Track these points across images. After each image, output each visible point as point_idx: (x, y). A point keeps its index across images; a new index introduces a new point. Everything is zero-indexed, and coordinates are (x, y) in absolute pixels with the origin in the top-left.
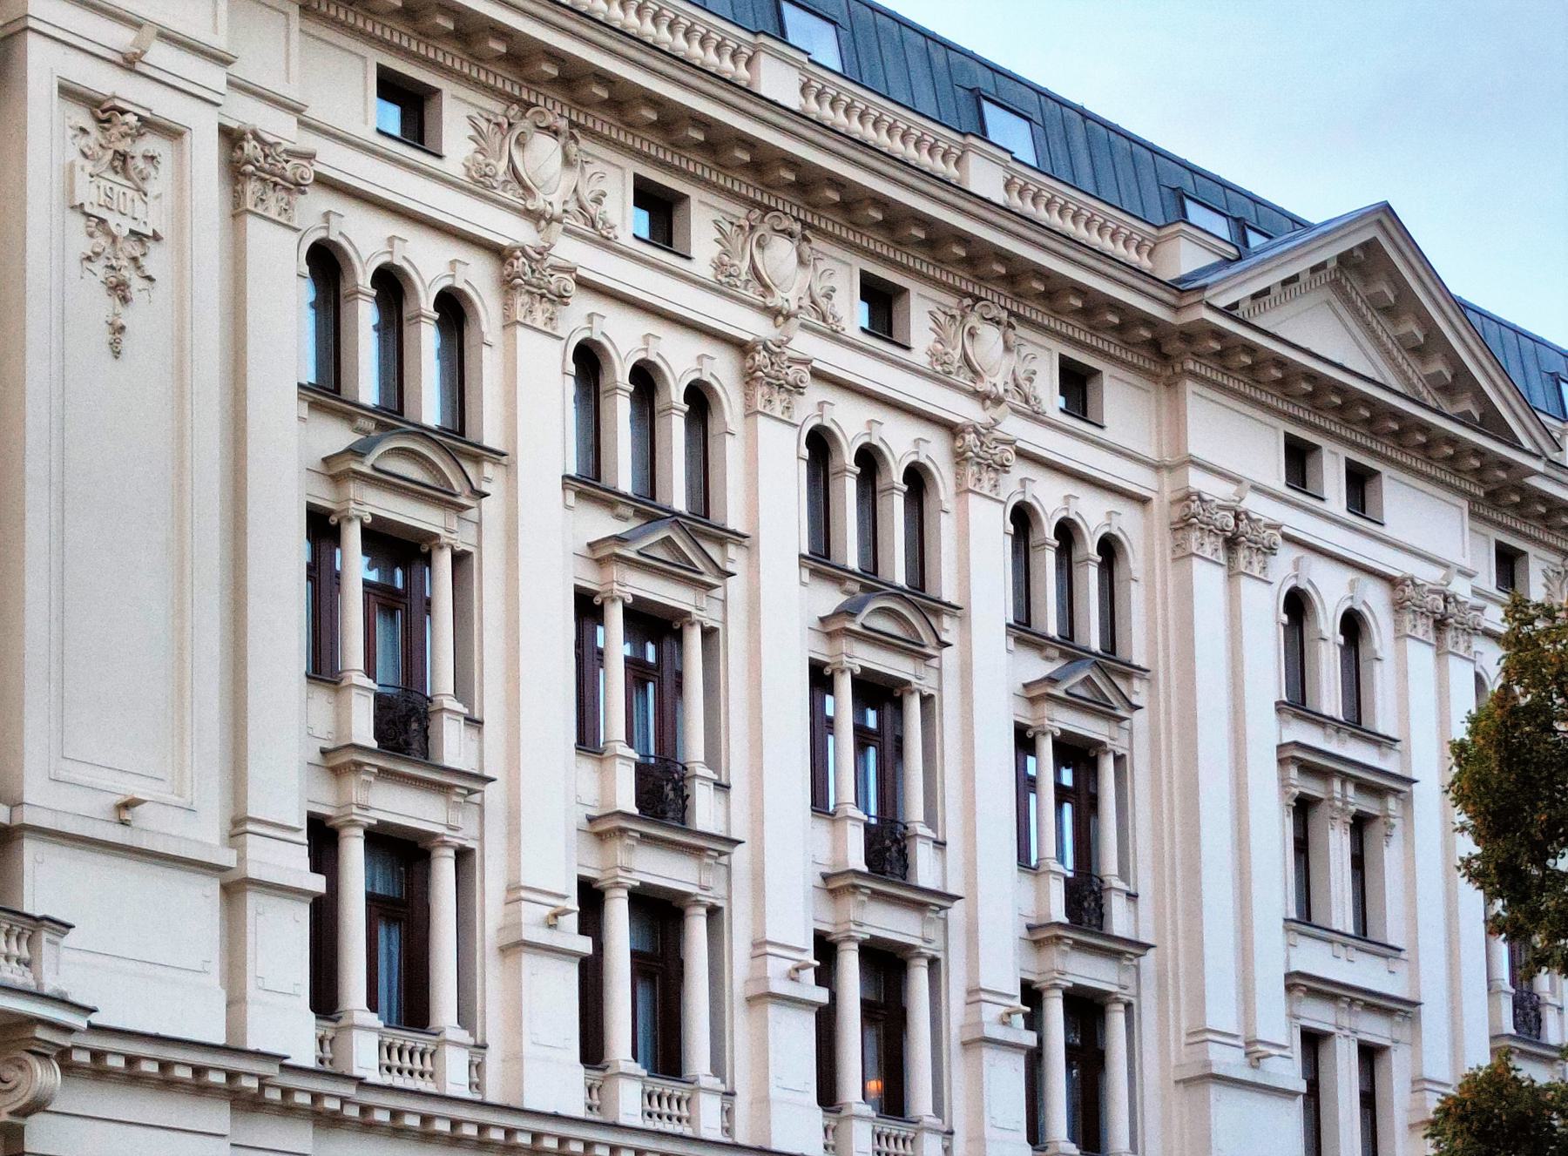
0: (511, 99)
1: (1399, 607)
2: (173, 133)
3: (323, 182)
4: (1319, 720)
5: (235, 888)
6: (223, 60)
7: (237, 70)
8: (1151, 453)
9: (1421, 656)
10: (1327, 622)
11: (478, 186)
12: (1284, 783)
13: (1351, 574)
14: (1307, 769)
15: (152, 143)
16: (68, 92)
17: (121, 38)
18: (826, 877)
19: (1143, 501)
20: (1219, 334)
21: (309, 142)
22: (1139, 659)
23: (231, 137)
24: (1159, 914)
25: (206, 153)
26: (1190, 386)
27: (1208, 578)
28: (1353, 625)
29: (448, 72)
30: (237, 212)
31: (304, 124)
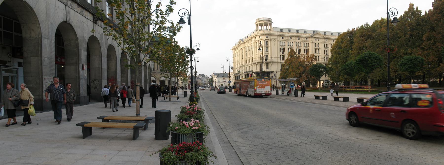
11: (285, 39)
25: (277, 40)
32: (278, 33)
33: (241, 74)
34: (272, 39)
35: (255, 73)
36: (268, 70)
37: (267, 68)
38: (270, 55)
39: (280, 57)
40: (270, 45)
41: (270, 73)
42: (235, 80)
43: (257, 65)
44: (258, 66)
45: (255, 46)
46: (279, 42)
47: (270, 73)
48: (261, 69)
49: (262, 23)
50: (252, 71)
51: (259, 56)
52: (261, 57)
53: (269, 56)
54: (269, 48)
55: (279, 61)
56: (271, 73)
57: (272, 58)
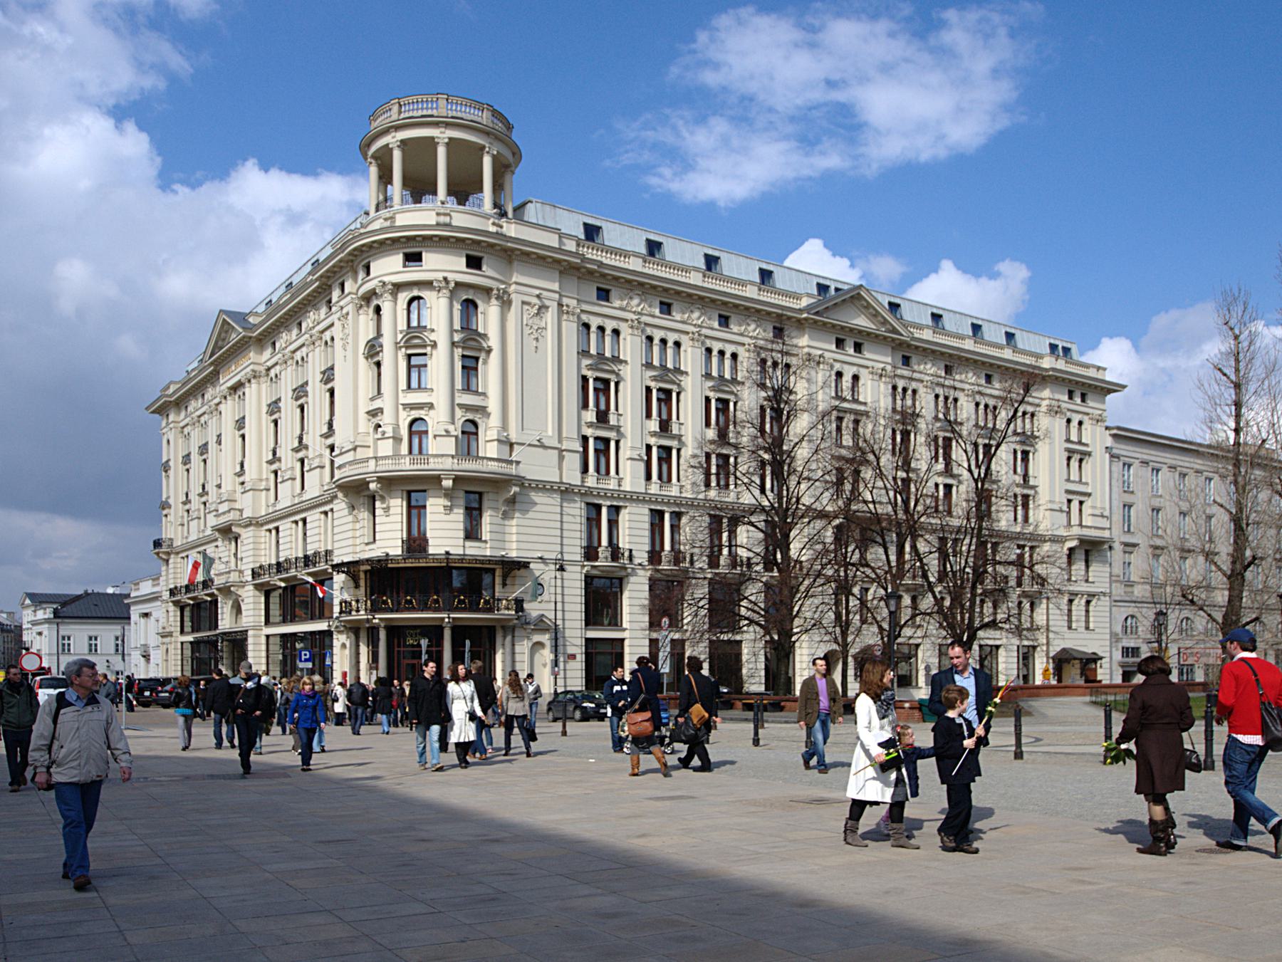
32: (571, 246)
33: (226, 590)
35: (350, 568)
36: (473, 549)
37: (472, 533)
40: (494, 342)
41: (498, 573)
42: (182, 632)
43: (378, 504)
44: (387, 509)
46: (570, 329)
47: (493, 571)
48: (415, 543)
49: (431, 143)
50: (328, 553)
51: (396, 427)
52: (411, 433)
53: (489, 431)
54: (485, 362)
56: (505, 577)
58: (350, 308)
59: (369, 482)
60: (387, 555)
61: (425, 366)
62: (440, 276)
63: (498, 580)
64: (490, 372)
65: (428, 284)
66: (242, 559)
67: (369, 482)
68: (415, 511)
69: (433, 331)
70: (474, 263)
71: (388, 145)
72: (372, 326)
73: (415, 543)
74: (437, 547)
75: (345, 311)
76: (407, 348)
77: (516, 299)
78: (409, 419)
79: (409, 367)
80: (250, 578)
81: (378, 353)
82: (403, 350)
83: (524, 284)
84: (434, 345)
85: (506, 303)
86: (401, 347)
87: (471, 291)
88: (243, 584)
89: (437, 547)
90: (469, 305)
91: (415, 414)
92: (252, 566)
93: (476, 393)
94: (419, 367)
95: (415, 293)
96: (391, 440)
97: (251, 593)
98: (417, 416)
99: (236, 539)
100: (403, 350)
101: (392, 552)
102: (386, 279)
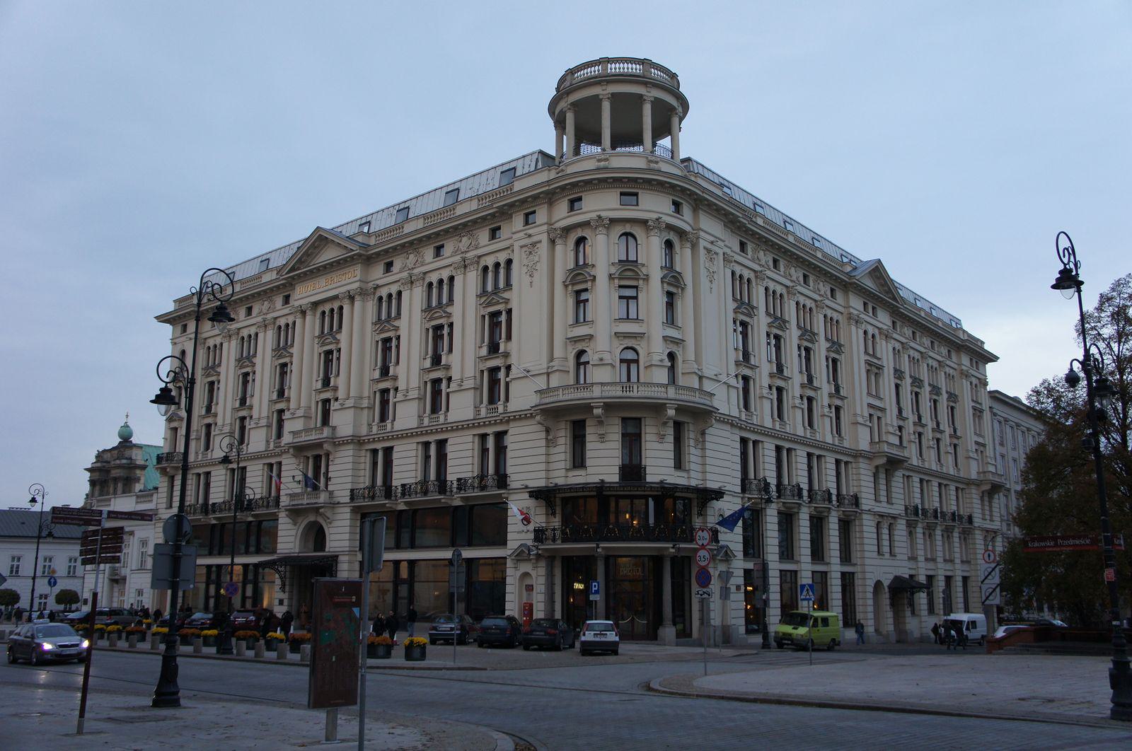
0: (757, 244)
1: (880, 333)
2: (716, 254)
3: (735, 261)
4: (869, 354)
5: (729, 386)
6: (724, 241)
7: (726, 243)
8: (843, 305)
9: (884, 342)
10: (870, 336)
12: (866, 367)
13: (873, 327)
14: (870, 365)
15: (715, 256)
16: (705, 248)
17: (712, 239)
18: (801, 384)
19: (842, 313)
20: (856, 283)
21: (732, 254)
22: (842, 343)
23: (724, 254)
24: (847, 390)
26: (850, 293)
27: (853, 328)
28: (873, 336)
29: (749, 240)
30: (724, 267)
31: (732, 251)
34: (702, 234)
37: (679, 465)
38: (691, 355)
39: (733, 382)
41: (695, 503)
45: (559, 277)
48: (632, 470)
52: (622, 361)
55: (735, 413)
57: (705, 381)
58: (544, 238)
59: (592, 408)
60: (602, 481)
61: (636, 298)
62: (655, 216)
63: (695, 510)
64: (685, 307)
65: (644, 223)
66: (328, 479)
67: (592, 408)
68: (632, 441)
69: (643, 265)
70: (677, 205)
71: (598, 95)
72: (571, 255)
73: (632, 470)
74: (653, 476)
75: (535, 239)
76: (620, 279)
77: (702, 243)
78: (623, 347)
79: (620, 297)
80: (349, 501)
81: (586, 281)
82: (616, 281)
83: (710, 227)
84: (647, 278)
85: (694, 246)
86: (613, 279)
87: (672, 233)
88: (334, 505)
89: (653, 476)
90: (669, 244)
91: (630, 343)
92: (349, 486)
93: (678, 328)
94: (628, 298)
95: (629, 230)
96: (609, 367)
97: (348, 516)
98: (630, 345)
99: (317, 459)
100: (616, 281)
101: (608, 479)
102: (604, 214)
